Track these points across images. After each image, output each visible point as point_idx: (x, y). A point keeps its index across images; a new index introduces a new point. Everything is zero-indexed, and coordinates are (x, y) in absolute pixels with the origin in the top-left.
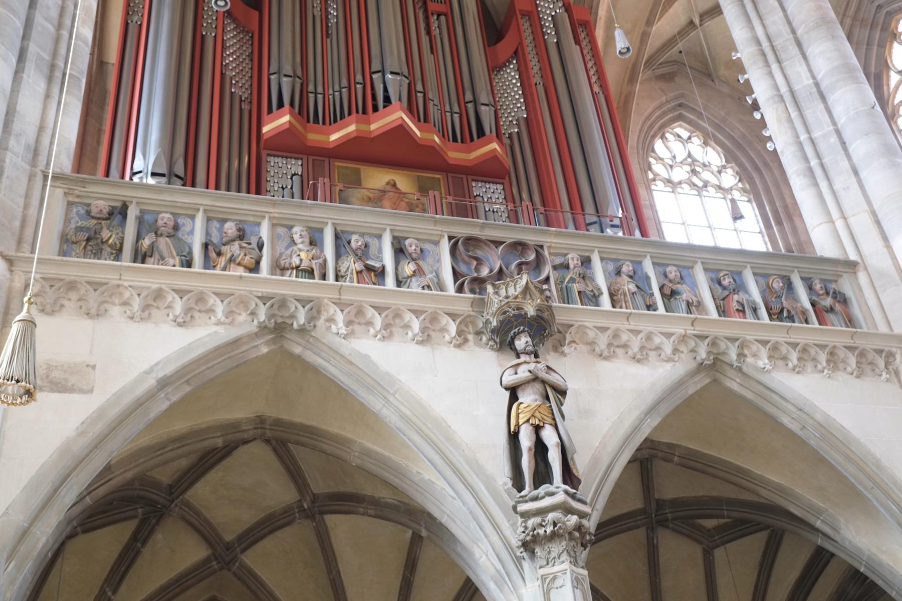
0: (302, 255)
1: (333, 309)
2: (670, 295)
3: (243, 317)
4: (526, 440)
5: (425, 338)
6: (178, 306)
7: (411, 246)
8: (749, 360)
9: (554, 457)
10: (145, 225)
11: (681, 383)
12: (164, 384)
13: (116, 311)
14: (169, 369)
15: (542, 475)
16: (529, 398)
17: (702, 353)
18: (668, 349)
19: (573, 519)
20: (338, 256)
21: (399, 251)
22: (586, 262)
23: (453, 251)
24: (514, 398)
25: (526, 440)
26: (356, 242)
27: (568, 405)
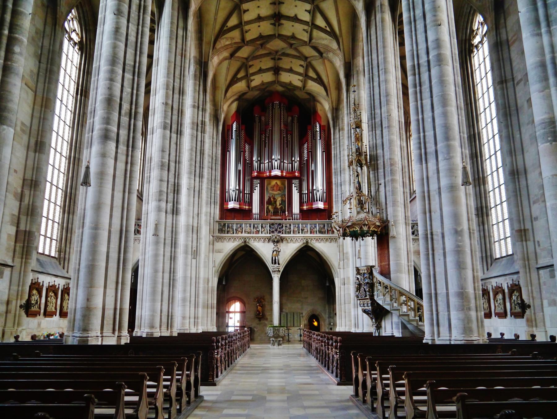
0: (248, 229)
1: (251, 239)
2: (302, 230)
3: (240, 241)
4: (274, 259)
5: (264, 242)
6: (232, 240)
7: (264, 225)
8: (312, 241)
9: (277, 261)
10: (228, 227)
11: (301, 246)
12: (231, 251)
13: (225, 241)
14: (232, 249)
15: (275, 263)
16: (275, 253)
17: (305, 241)
18: (299, 241)
19: (277, 269)
20: (253, 228)
21: (262, 227)
22: (290, 225)
23: (270, 226)
24: (273, 252)
25: (274, 259)
26: (256, 226)
27: (280, 253)
